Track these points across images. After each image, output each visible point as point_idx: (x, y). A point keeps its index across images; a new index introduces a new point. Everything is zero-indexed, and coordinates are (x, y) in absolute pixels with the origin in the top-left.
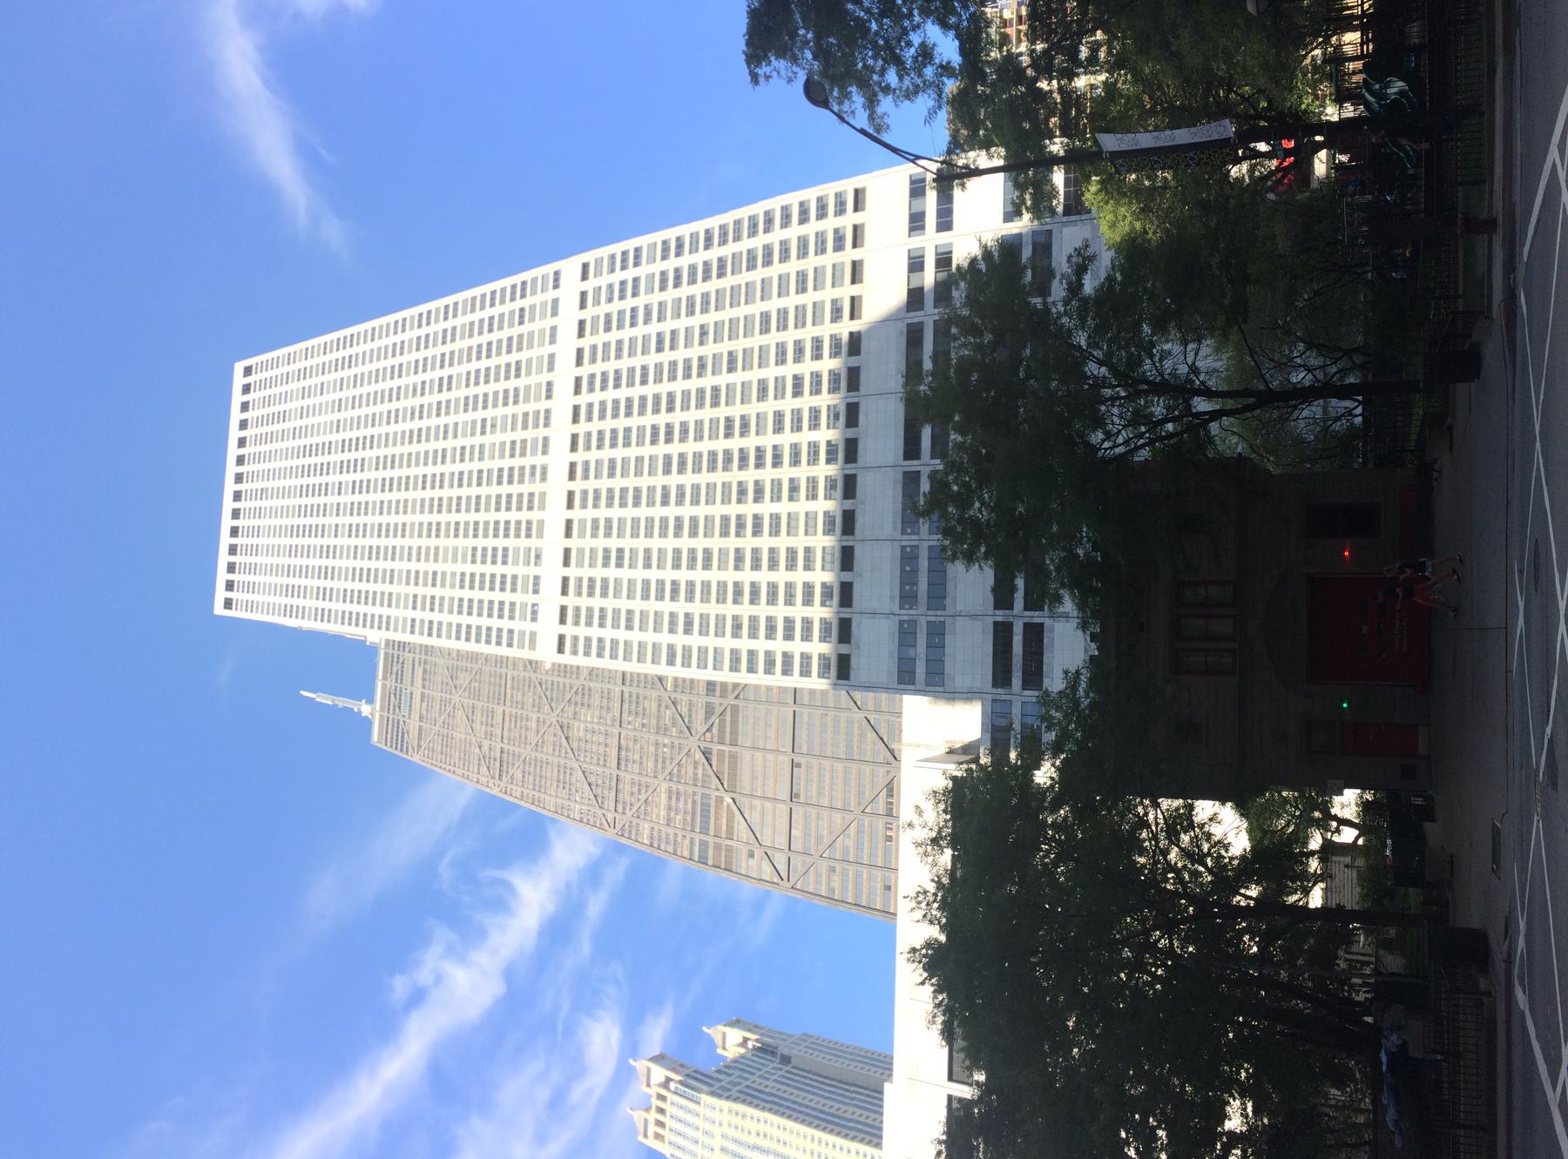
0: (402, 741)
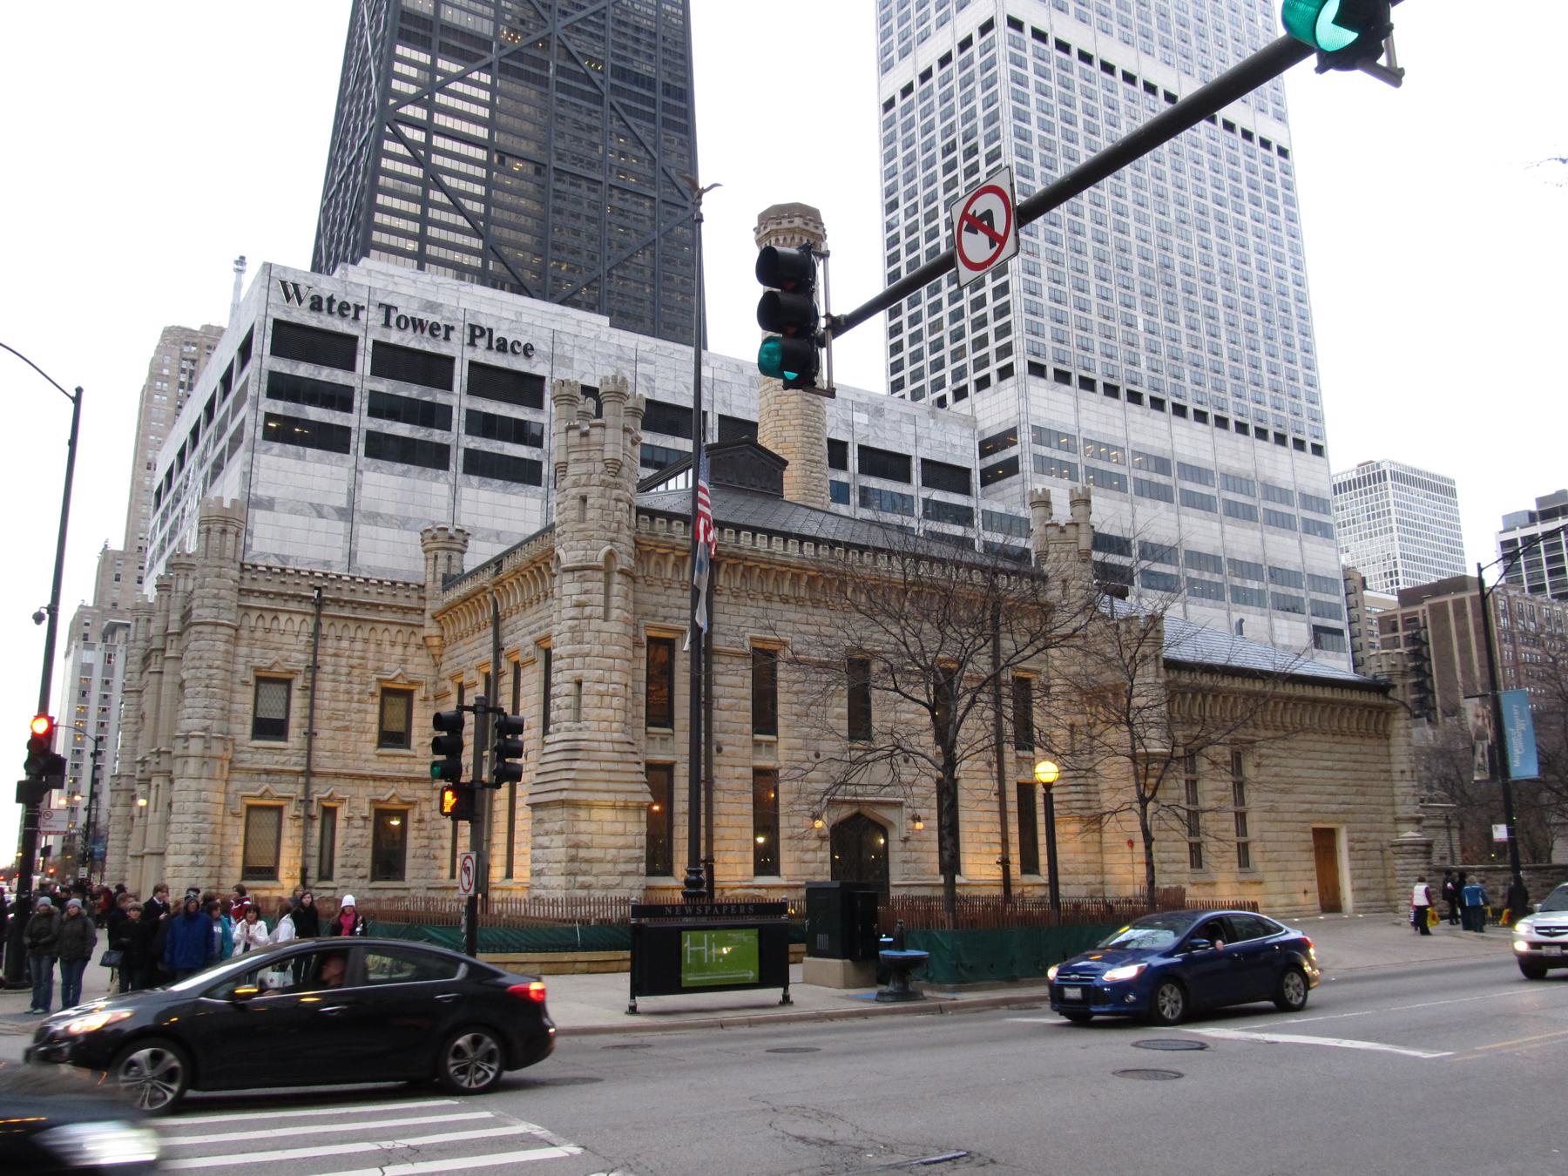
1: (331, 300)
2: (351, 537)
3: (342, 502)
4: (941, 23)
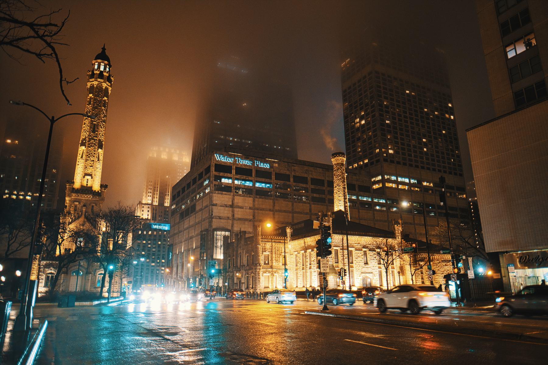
2: (233, 211)
3: (231, 203)
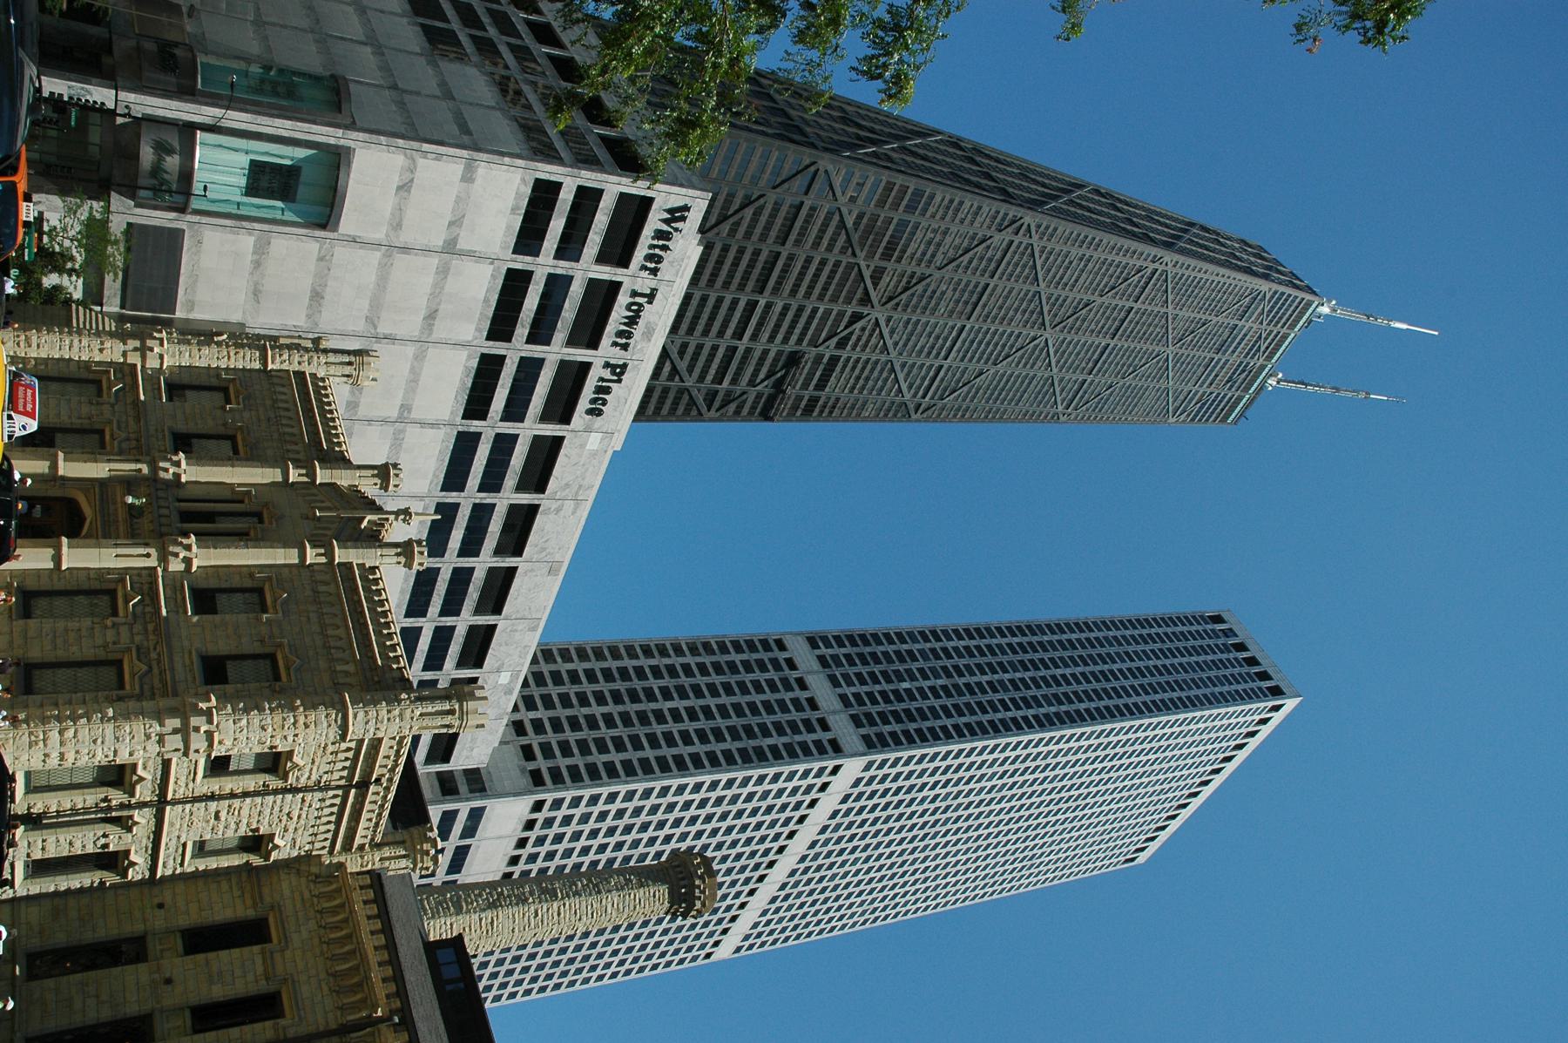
0: (1273, 307)
1: (665, 248)
2: (427, 251)
3: (462, 245)
4: (843, 698)
